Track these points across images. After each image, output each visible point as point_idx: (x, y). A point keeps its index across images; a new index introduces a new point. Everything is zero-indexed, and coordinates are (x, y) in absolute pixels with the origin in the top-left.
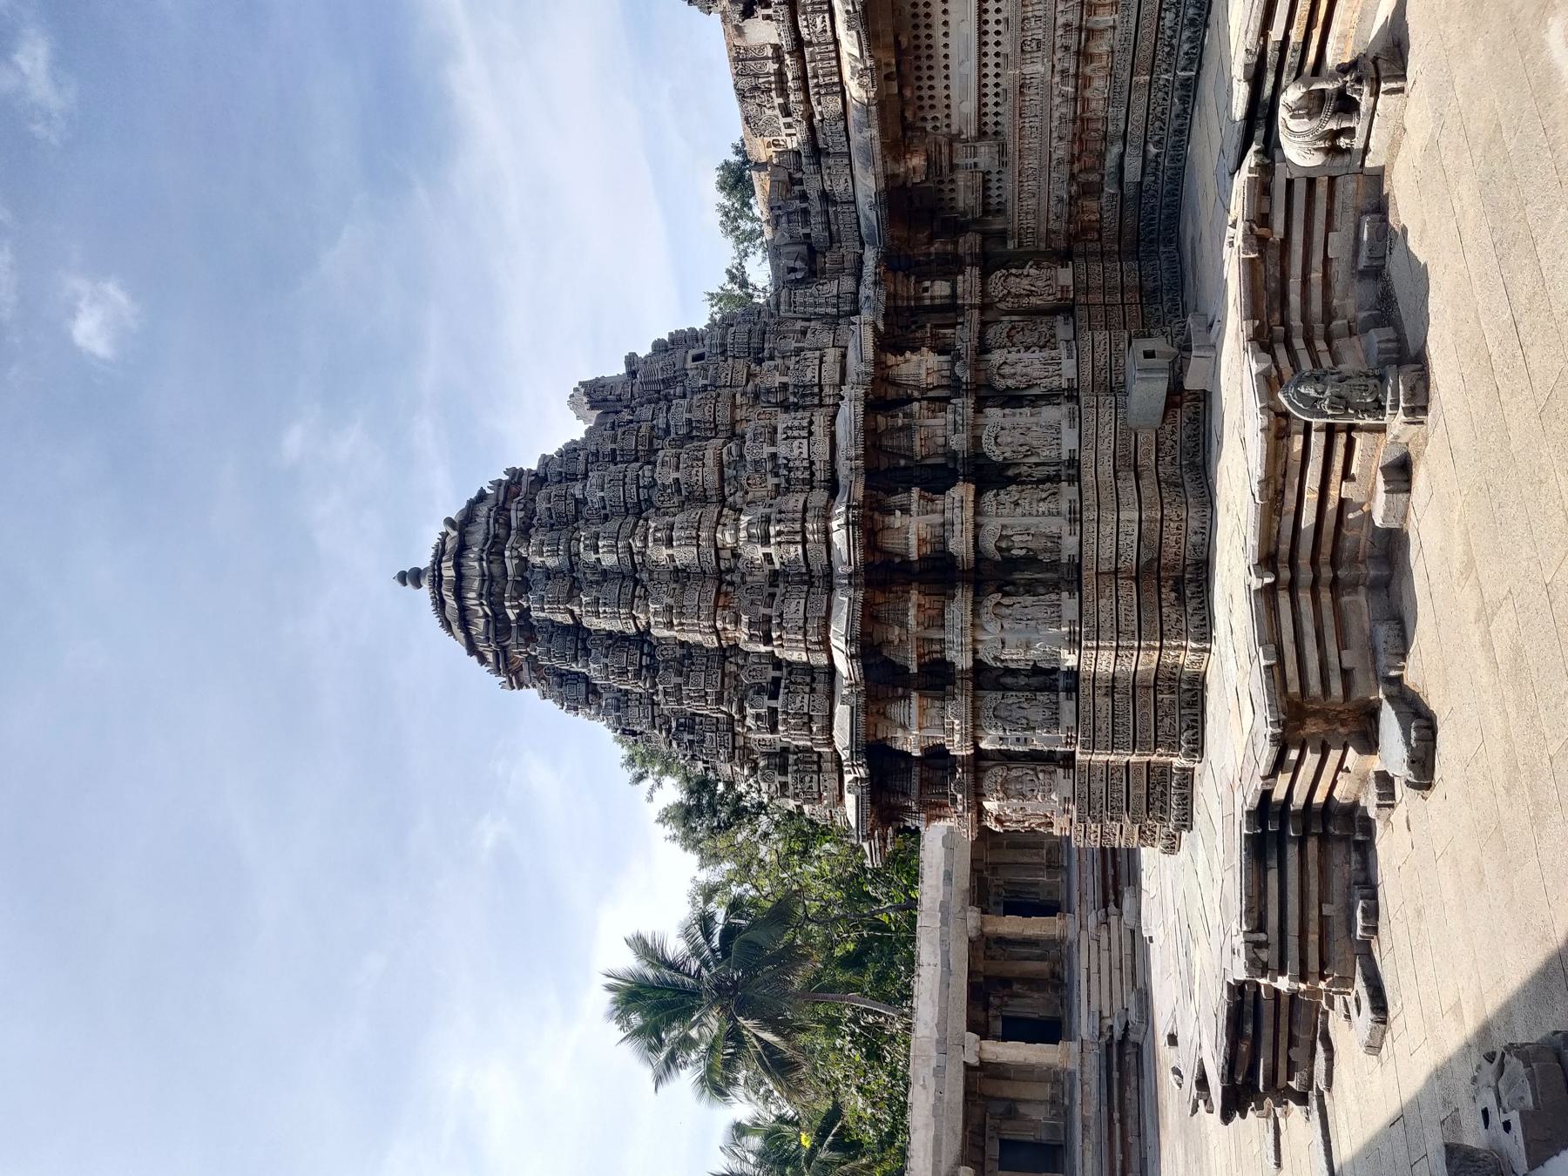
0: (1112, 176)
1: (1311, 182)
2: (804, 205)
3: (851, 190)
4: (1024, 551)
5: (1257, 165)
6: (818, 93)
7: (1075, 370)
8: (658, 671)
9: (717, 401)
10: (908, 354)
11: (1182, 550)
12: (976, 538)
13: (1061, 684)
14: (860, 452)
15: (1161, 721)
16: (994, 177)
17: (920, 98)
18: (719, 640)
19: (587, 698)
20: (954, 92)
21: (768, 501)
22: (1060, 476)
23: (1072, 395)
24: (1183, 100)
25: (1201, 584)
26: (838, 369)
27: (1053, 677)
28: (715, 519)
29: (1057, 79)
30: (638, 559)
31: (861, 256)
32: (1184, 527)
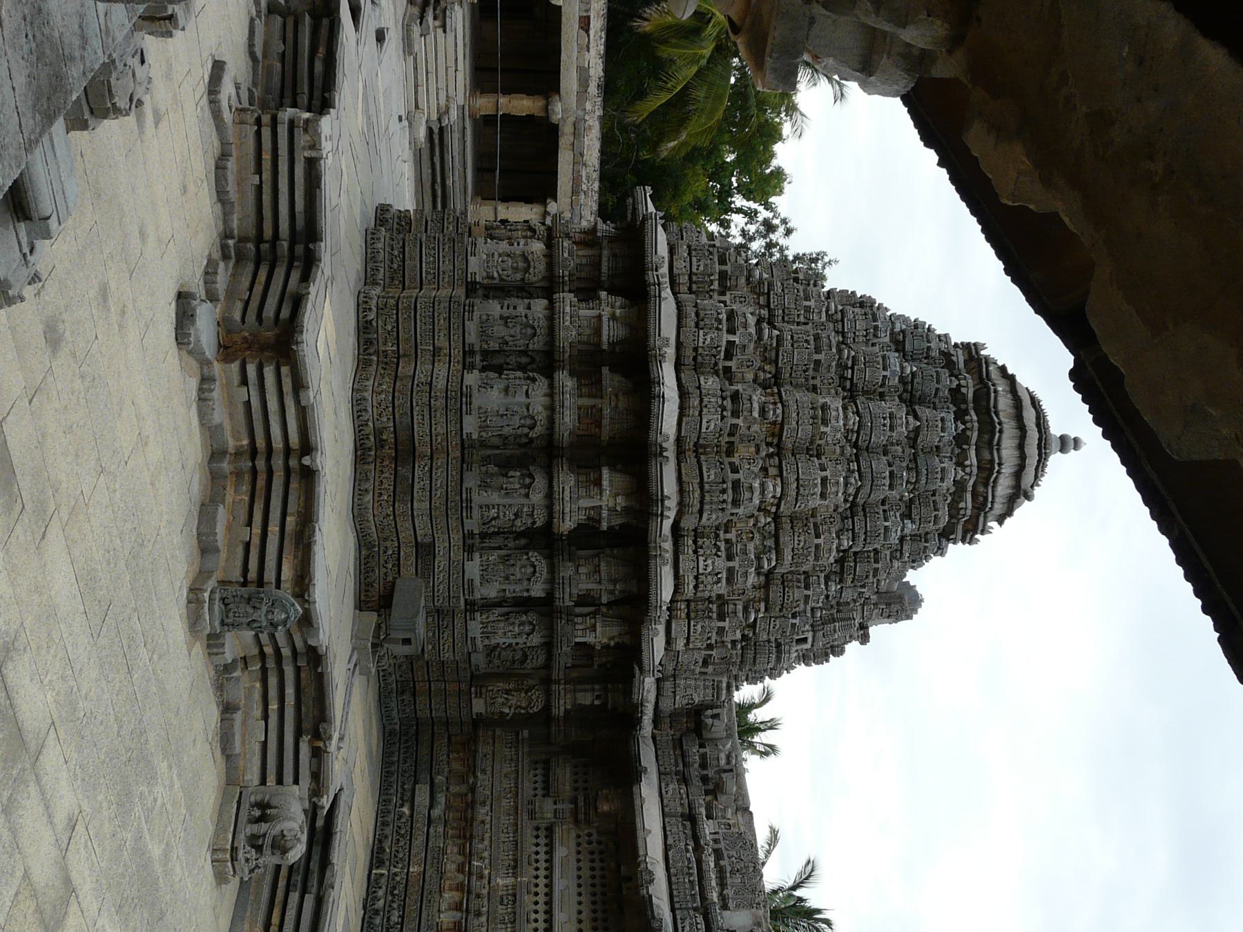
1: (280, 781)
2: (705, 772)
3: (663, 784)
4: (511, 473)
5: (322, 796)
6: (689, 868)
7: (468, 627)
8: (837, 365)
9: (782, 605)
10: (612, 643)
11: (377, 475)
12: (551, 486)
13: (478, 358)
15: (394, 327)
16: (540, 792)
17: (602, 861)
18: (779, 393)
19: (904, 337)
21: (735, 519)
22: (480, 538)
23: (471, 607)
24: (381, 850)
25: (361, 445)
26: (673, 631)
27: (485, 363)
28: (783, 502)
29: (486, 872)
30: (854, 466)
31: (655, 727)
32: (376, 495)
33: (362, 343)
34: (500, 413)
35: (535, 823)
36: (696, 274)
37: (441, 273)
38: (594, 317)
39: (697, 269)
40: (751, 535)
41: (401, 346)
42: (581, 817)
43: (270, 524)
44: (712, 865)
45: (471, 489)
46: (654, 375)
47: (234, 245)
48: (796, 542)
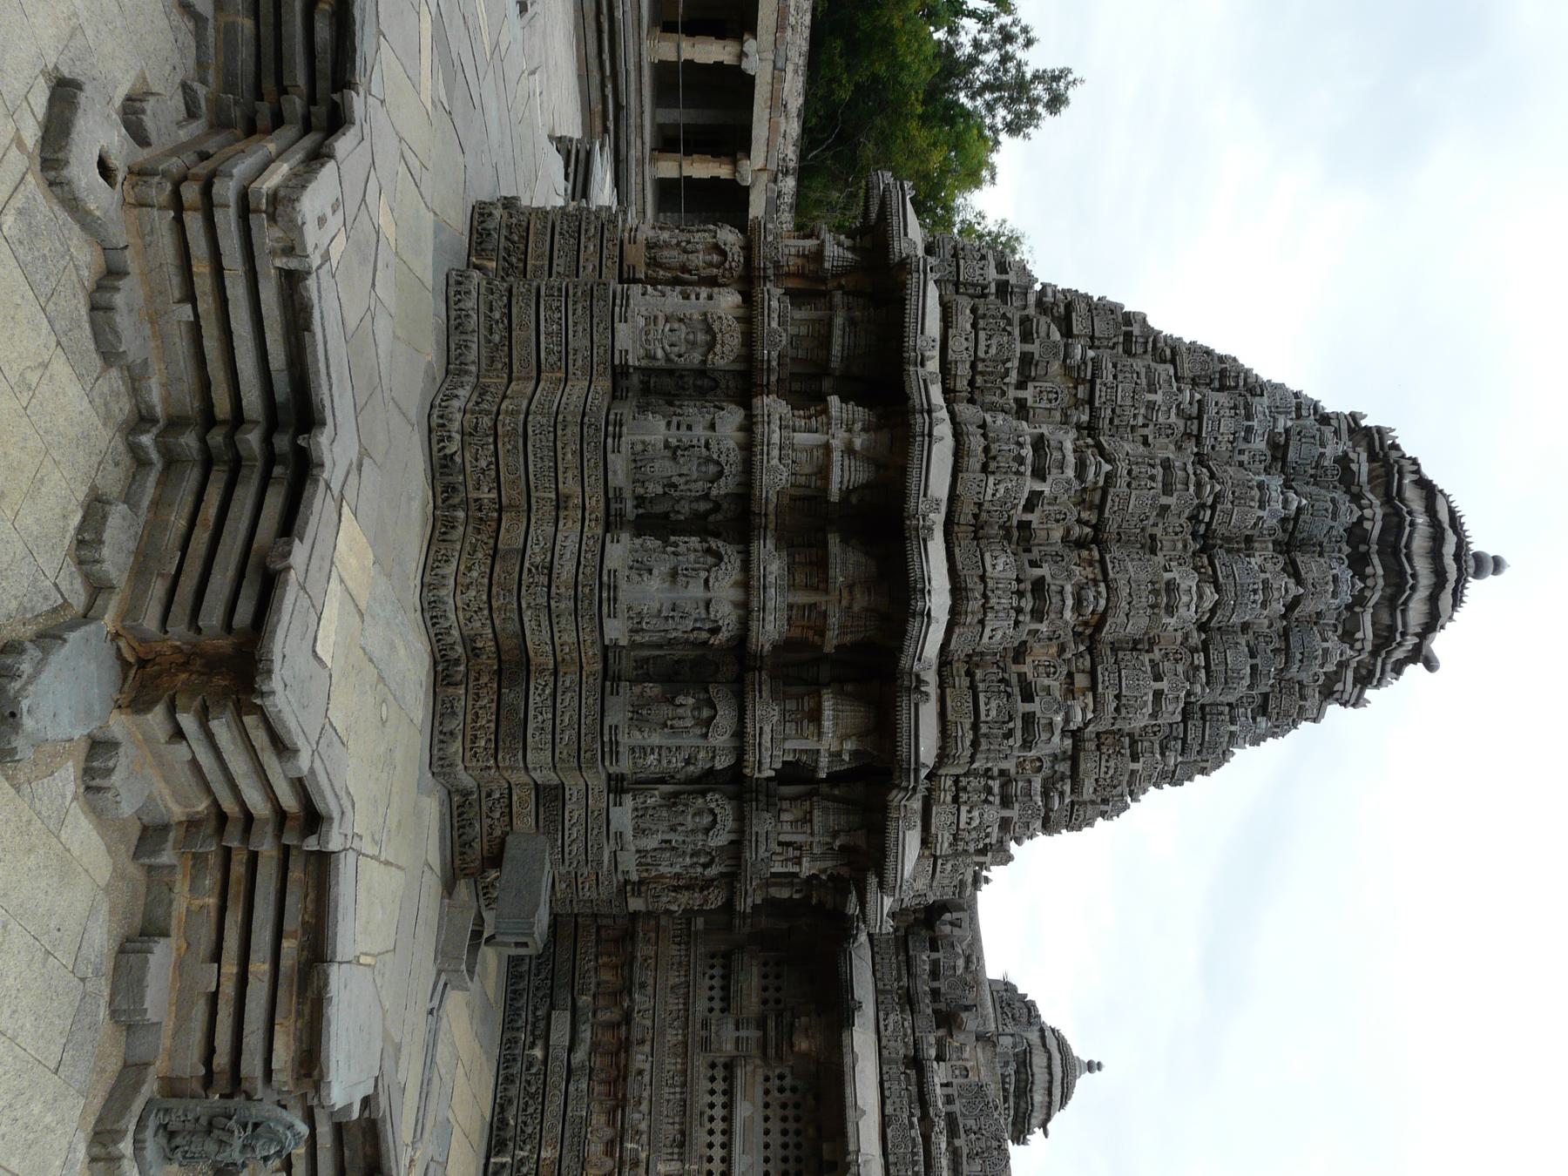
0: (584, 1018)
3: (881, 1014)
4: (680, 700)
11: (470, 703)
14: (892, 825)
15: (490, 463)
16: (717, 1005)
17: (797, 1119)
18: (1102, 561)
19: (1287, 440)
20: (760, 1126)
24: (503, 1123)
27: (641, 511)
29: (643, 1155)
30: (1200, 659)
32: (468, 738)
33: (439, 489)
34: (664, 614)
35: (710, 1057)
36: (984, 360)
37: (571, 352)
38: (818, 447)
39: (986, 352)
40: (1038, 764)
41: (503, 493)
42: (772, 1052)
43: (253, 957)
44: (944, 1146)
45: (616, 727)
46: (914, 574)
47: (155, 441)
48: (1103, 769)
